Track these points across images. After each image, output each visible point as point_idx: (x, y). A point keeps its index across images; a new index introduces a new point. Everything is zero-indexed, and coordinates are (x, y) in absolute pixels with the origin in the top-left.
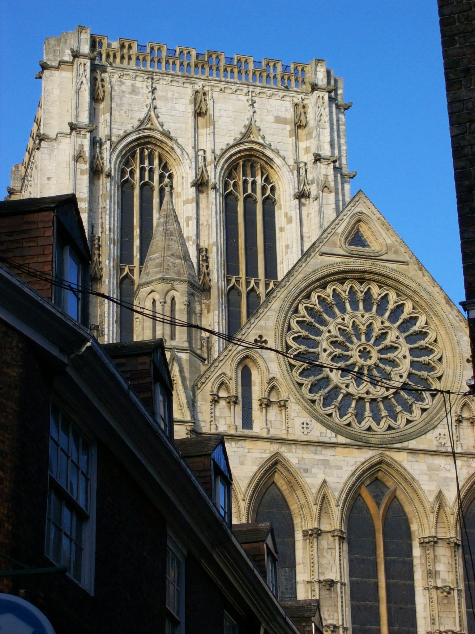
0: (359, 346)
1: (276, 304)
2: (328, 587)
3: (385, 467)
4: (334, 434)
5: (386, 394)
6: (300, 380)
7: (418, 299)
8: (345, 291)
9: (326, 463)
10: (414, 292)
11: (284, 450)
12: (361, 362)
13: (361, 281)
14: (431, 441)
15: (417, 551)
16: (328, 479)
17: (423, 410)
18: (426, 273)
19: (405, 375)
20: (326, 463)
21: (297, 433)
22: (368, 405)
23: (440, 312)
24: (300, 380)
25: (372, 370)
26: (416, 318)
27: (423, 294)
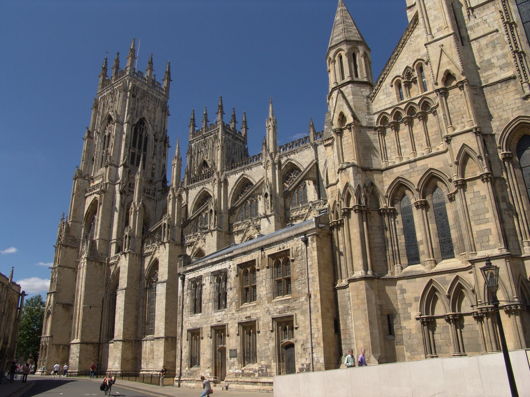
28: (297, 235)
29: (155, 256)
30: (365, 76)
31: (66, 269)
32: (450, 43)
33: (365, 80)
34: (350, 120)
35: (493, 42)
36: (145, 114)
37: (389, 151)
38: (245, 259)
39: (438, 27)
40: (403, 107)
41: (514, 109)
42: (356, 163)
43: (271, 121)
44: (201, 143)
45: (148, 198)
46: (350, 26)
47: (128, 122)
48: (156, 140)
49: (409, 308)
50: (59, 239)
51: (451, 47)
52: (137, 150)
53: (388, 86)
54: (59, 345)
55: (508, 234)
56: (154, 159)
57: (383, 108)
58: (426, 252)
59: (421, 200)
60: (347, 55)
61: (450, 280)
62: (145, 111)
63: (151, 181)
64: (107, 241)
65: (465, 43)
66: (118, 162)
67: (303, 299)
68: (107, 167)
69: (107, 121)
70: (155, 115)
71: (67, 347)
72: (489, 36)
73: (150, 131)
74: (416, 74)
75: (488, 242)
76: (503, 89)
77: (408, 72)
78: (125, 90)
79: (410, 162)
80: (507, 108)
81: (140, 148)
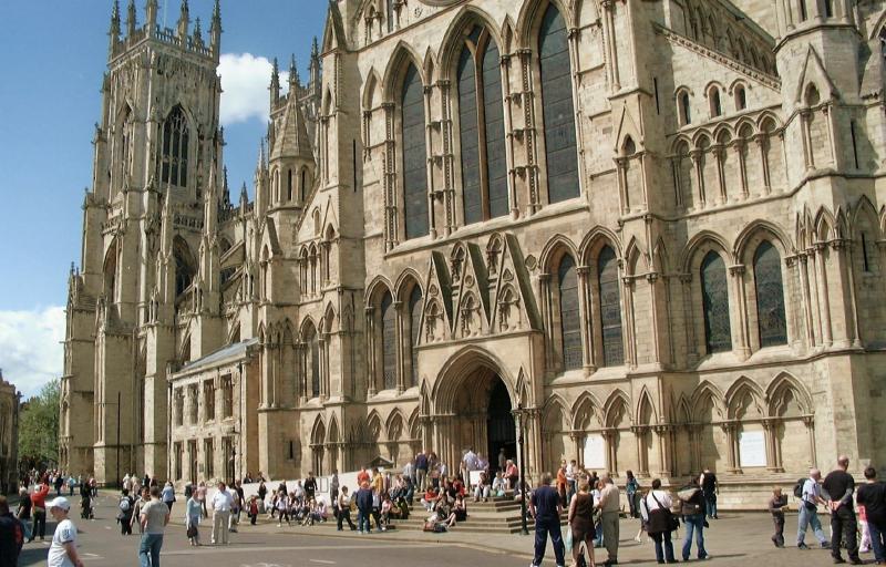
20: (430, 34)
21: (414, 20)
29: (191, 330)
31: (83, 344)
34: (271, 255)
35: (374, 192)
36: (181, 98)
38: (208, 376)
40: (317, 242)
45: (192, 231)
47: (152, 120)
48: (201, 137)
50: (70, 301)
52: (171, 159)
54: (83, 448)
56: (200, 170)
60: (282, 173)
62: (181, 94)
63: (196, 206)
64: (132, 304)
66: (142, 184)
67: (238, 422)
68: (125, 192)
69: (124, 113)
70: (197, 96)
71: (91, 450)
73: (191, 125)
78: (146, 66)
79: (316, 302)
81: (176, 154)
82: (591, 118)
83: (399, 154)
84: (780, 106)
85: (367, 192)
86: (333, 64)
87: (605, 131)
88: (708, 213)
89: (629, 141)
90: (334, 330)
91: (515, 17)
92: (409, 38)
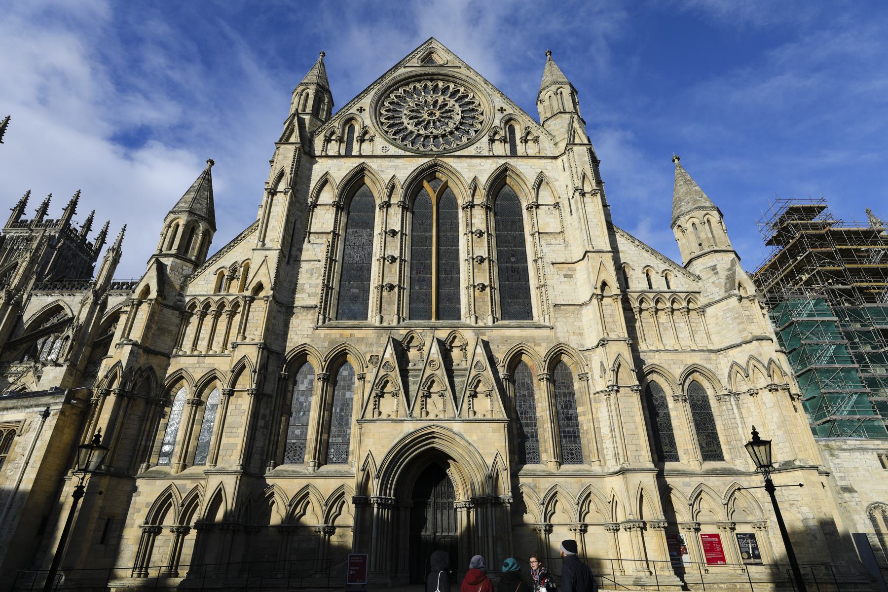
0: (428, 111)
1: (373, 92)
2: (391, 235)
3: (439, 168)
4: (403, 152)
5: (444, 132)
6: (394, 137)
7: (467, 85)
8: (421, 86)
9: (396, 167)
10: (464, 81)
11: (368, 161)
12: (430, 118)
13: (431, 80)
14: (471, 151)
15: (461, 214)
16: (396, 175)
17: (468, 139)
18: (471, 70)
19: (457, 123)
20: (396, 167)
21: (379, 153)
22: (432, 139)
23: (481, 88)
24: (386, 129)
25: (436, 123)
26: (467, 96)
27: (470, 81)
28: (37, 406)
30: (195, 254)
32: (273, 257)
33: (193, 258)
34: (153, 294)
37: (186, 338)
39: (272, 238)
40: (217, 298)
41: (305, 336)
42: (139, 342)
43: (113, 252)
44: (23, 239)
46: (204, 198)
49: (136, 514)
51: (273, 260)
53: (212, 273)
55: (254, 452)
57: (197, 294)
58: (178, 454)
59: (195, 398)
61: (189, 489)
65: (292, 261)
72: (312, 263)
74: (241, 271)
75: (230, 456)
76: (304, 314)
77: (234, 270)
79: (199, 356)
80: (299, 333)
82: (553, 264)
83: (340, 246)
84: (699, 293)
85: (304, 267)
86: (292, 154)
87: (565, 276)
88: (654, 351)
89: (604, 284)
90: (238, 387)
91: (484, 179)
92: (373, 164)
